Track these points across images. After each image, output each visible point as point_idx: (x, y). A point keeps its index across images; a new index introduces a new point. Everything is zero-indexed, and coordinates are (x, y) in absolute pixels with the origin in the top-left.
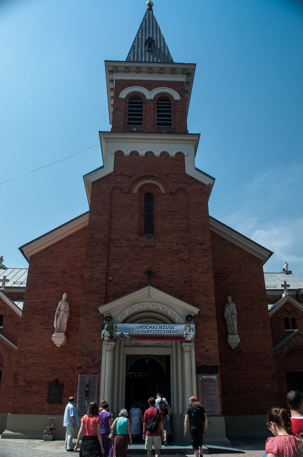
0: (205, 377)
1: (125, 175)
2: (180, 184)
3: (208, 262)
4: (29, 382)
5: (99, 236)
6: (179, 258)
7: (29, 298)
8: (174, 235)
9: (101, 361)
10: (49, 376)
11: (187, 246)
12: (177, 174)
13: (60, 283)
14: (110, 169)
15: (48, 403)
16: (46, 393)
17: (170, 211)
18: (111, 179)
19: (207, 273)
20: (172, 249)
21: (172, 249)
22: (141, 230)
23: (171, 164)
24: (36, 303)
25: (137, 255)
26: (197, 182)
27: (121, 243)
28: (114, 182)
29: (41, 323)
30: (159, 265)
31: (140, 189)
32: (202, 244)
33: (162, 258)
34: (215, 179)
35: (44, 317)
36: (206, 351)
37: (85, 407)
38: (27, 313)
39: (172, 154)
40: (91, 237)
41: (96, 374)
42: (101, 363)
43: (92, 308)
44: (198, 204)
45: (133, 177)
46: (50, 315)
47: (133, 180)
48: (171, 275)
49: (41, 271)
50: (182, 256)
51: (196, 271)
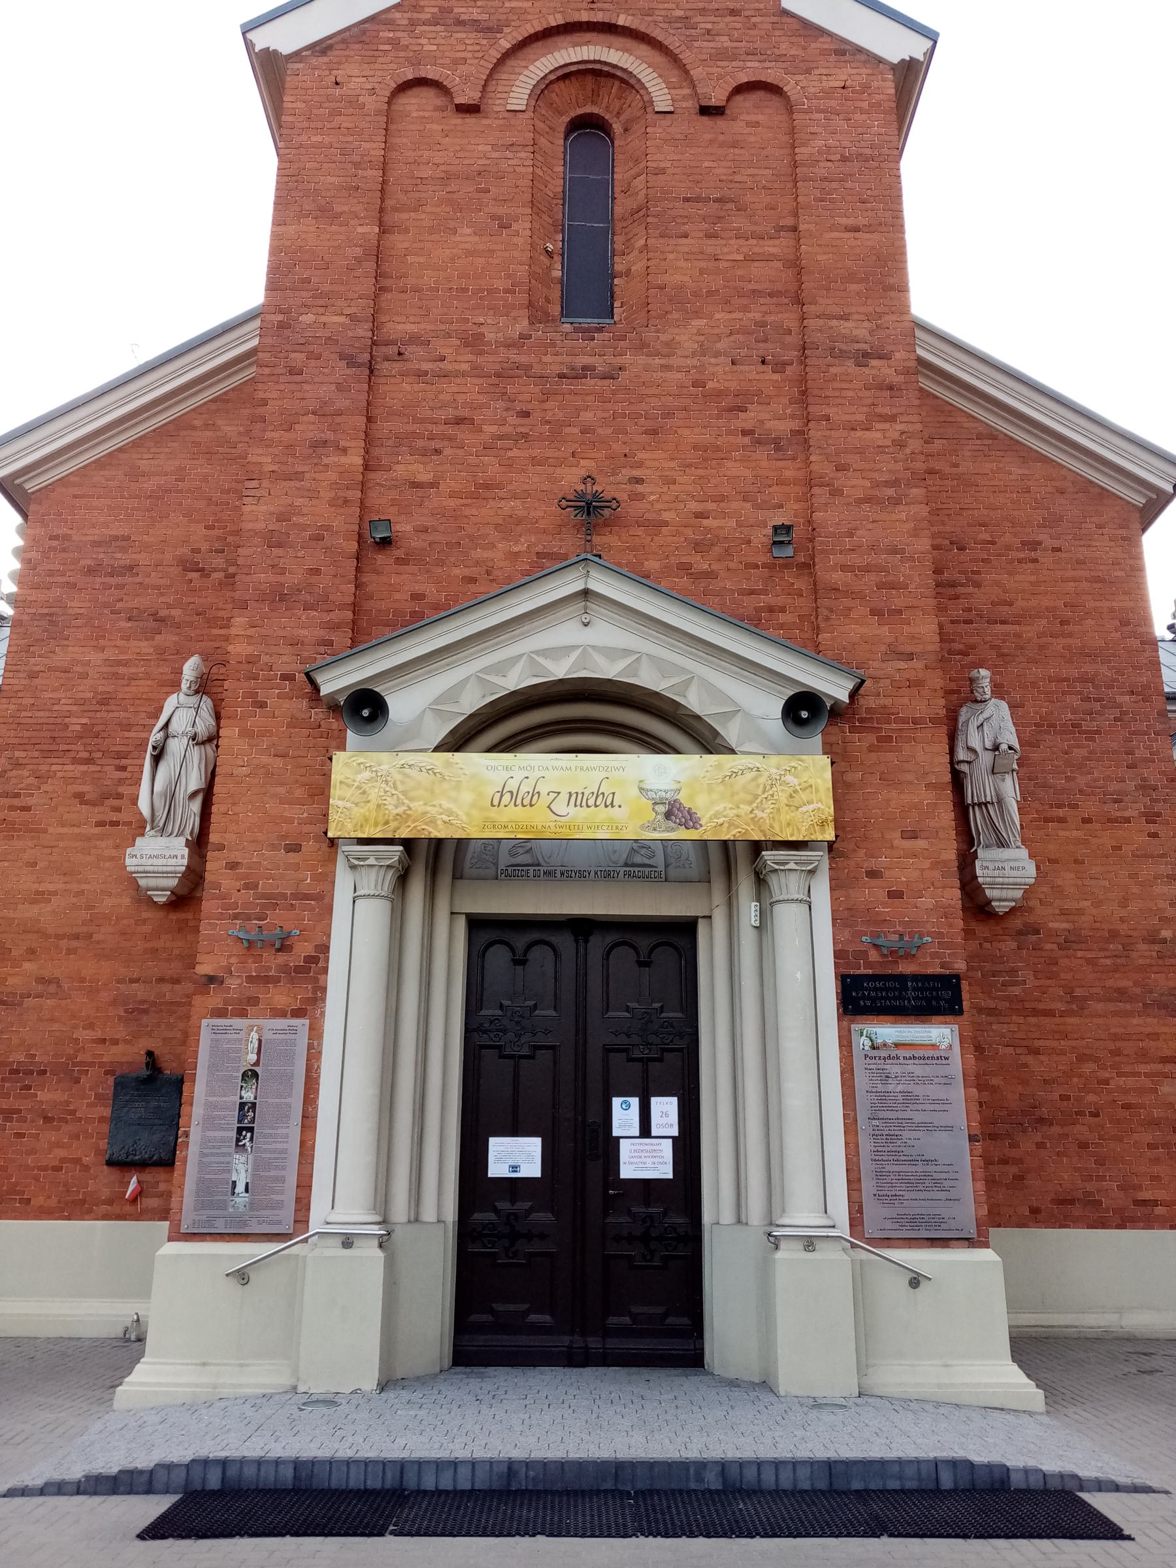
0: (888, 1032)
1: (460, 23)
2: (749, 64)
3: (900, 444)
4: (17, 1072)
5: (323, 319)
6: (745, 433)
7: (24, 682)
8: (717, 316)
9: (325, 949)
10: (115, 1042)
11: (790, 370)
12: (733, 12)
13: (176, 613)
15: (110, 1163)
16: (102, 1119)
17: (697, 200)
18: (389, 41)
20: (710, 385)
21: (710, 385)
22: (548, 301)
24: (56, 708)
25: (526, 414)
26: (846, 51)
27: (442, 359)
28: (402, 54)
29: (80, 797)
30: (640, 465)
31: (544, 89)
32: (866, 355)
33: (655, 432)
34: (937, 34)
35: (99, 768)
36: (892, 895)
37: (233, 1193)
38: (17, 754)
40: (282, 326)
41: (298, 1013)
42: (327, 960)
43: (284, 677)
44: (844, 159)
45: (506, 30)
46: (124, 762)
47: (506, 44)
48: (700, 515)
49: (83, 562)
50: (762, 422)
51: (836, 492)
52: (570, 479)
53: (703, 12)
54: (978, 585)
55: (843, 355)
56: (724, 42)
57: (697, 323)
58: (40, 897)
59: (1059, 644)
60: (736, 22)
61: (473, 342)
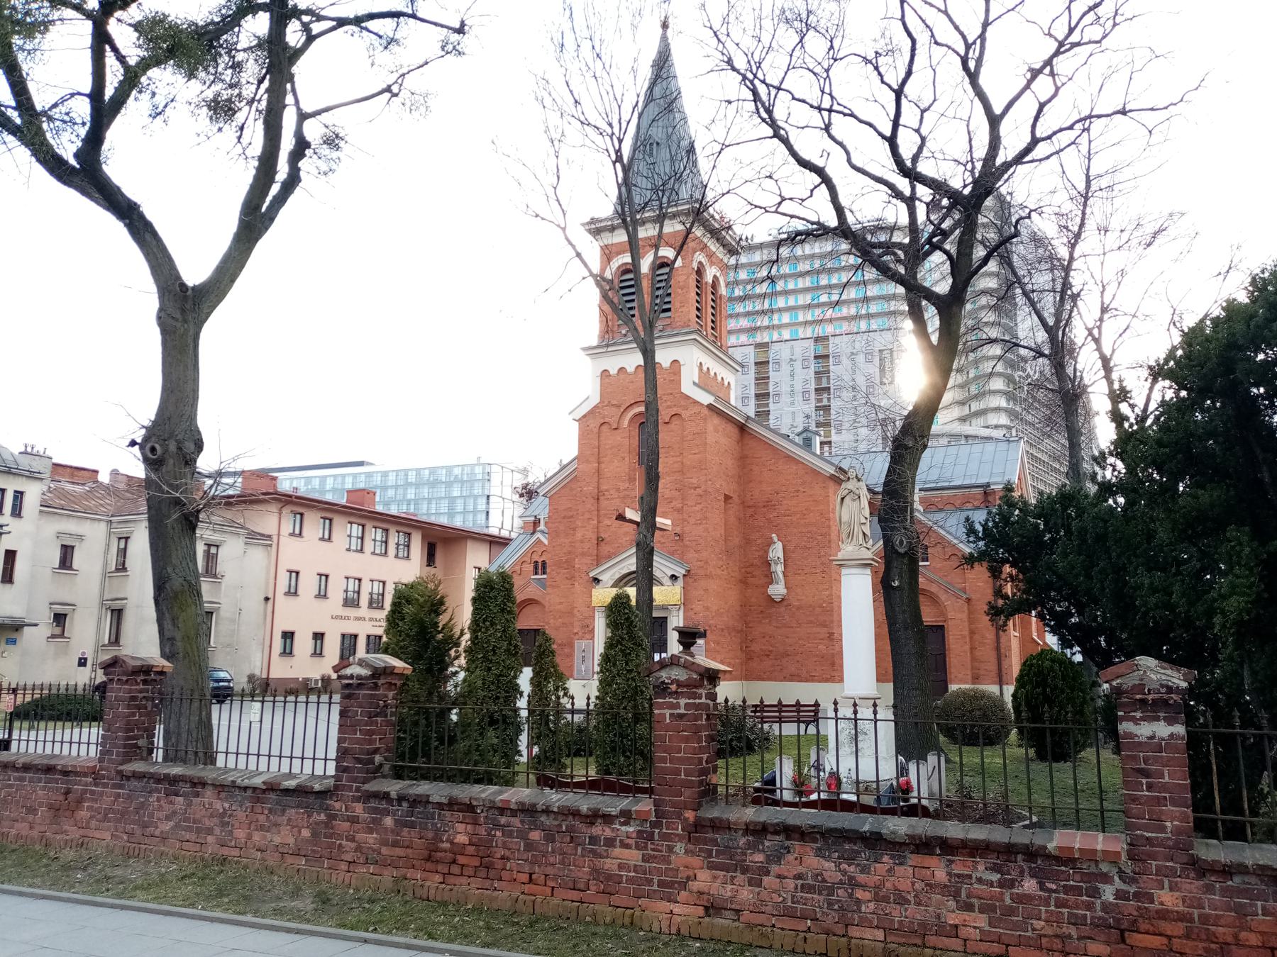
14: (596, 400)
26: (696, 402)
31: (631, 420)
56: (669, 403)
58: (561, 603)
59: (802, 522)
61: (618, 490)
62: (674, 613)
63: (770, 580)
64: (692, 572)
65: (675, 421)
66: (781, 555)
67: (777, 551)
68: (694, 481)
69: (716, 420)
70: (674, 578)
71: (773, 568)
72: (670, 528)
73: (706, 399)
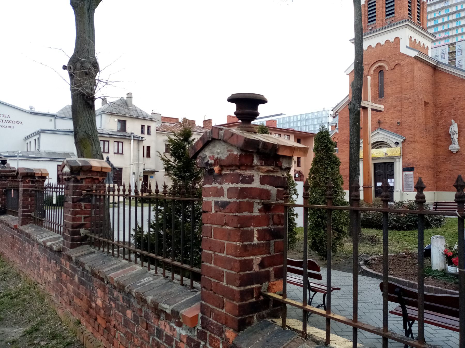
0: (407, 173)
3: (412, 110)
12: (395, 54)
19: (411, 117)
23: (391, 48)
26: (408, 56)
32: (408, 99)
39: (392, 40)
47: (370, 66)
52: (378, 118)
53: (391, 55)
54: (457, 105)
55: (406, 99)
56: (394, 59)
57: (391, 98)
58: (345, 159)
60: (395, 56)
62: (397, 160)
63: (450, 142)
64: (407, 140)
65: (397, 67)
66: (456, 129)
67: (454, 128)
68: (408, 96)
69: (419, 65)
70: (397, 143)
71: (452, 137)
72: (383, 110)
73: (413, 54)
